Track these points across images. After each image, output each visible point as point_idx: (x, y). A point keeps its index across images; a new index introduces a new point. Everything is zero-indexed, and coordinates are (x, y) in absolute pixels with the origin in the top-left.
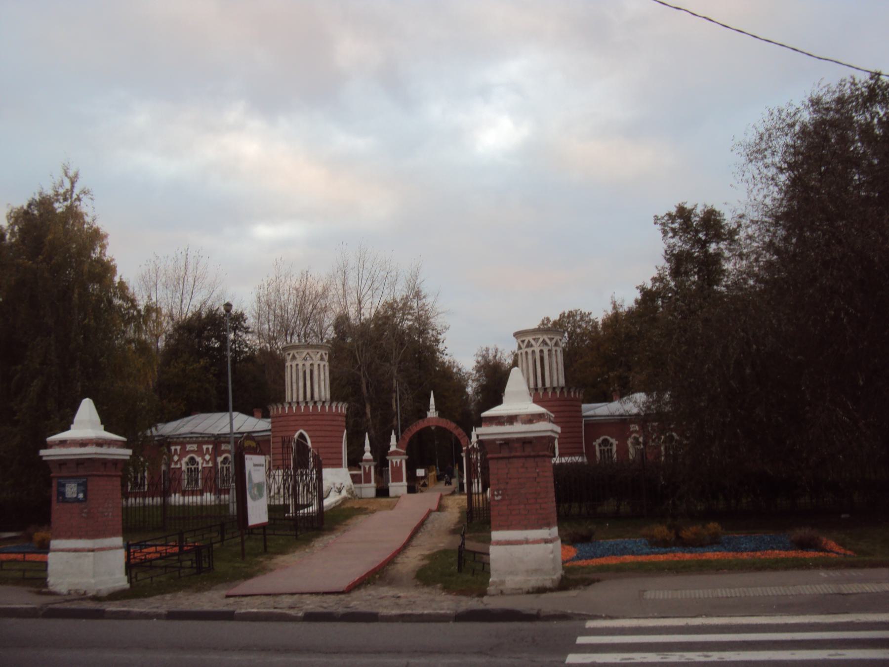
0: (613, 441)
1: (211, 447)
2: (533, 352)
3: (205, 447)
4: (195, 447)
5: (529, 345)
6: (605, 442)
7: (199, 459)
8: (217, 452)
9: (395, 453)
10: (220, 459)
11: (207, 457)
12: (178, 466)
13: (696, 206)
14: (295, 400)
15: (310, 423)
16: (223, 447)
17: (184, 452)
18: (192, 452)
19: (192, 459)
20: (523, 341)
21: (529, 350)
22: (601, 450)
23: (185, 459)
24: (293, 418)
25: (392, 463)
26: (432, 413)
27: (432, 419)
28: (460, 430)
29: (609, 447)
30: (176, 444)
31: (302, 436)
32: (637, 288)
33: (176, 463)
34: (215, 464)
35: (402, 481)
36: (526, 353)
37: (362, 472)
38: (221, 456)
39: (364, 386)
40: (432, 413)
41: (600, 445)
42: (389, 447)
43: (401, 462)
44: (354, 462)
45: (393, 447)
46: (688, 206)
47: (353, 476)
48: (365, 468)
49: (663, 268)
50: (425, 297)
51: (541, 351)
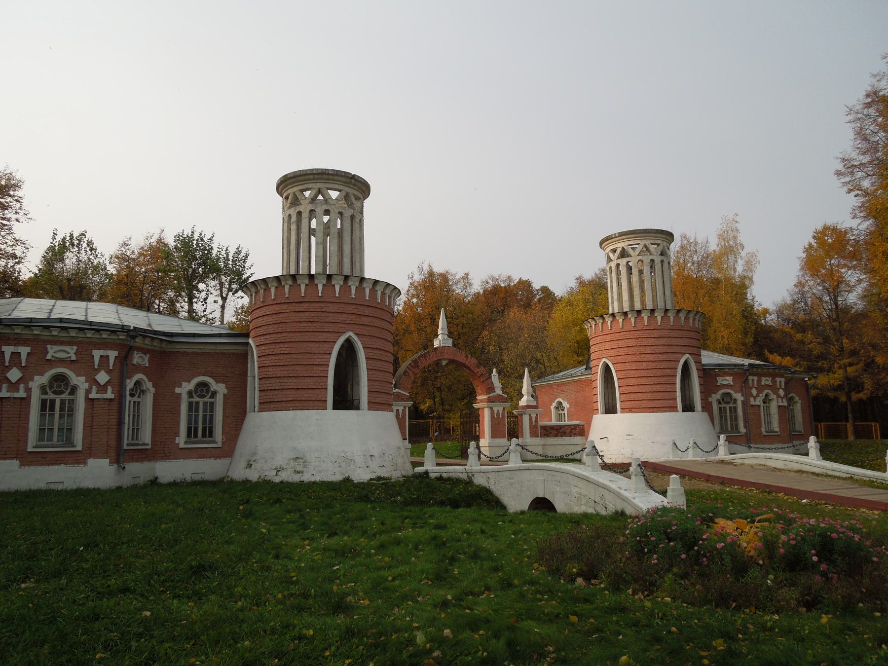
1: (113, 354)
2: (652, 261)
3: (97, 354)
4: (71, 352)
7: (80, 381)
8: (124, 366)
11: (102, 377)
12: (22, 394)
15: (365, 321)
17: (39, 362)
18: (62, 362)
19: (60, 379)
20: (614, 251)
23: (43, 379)
27: (442, 349)
30: (19, 341)
31: (349, 343)
33: (14, 386)
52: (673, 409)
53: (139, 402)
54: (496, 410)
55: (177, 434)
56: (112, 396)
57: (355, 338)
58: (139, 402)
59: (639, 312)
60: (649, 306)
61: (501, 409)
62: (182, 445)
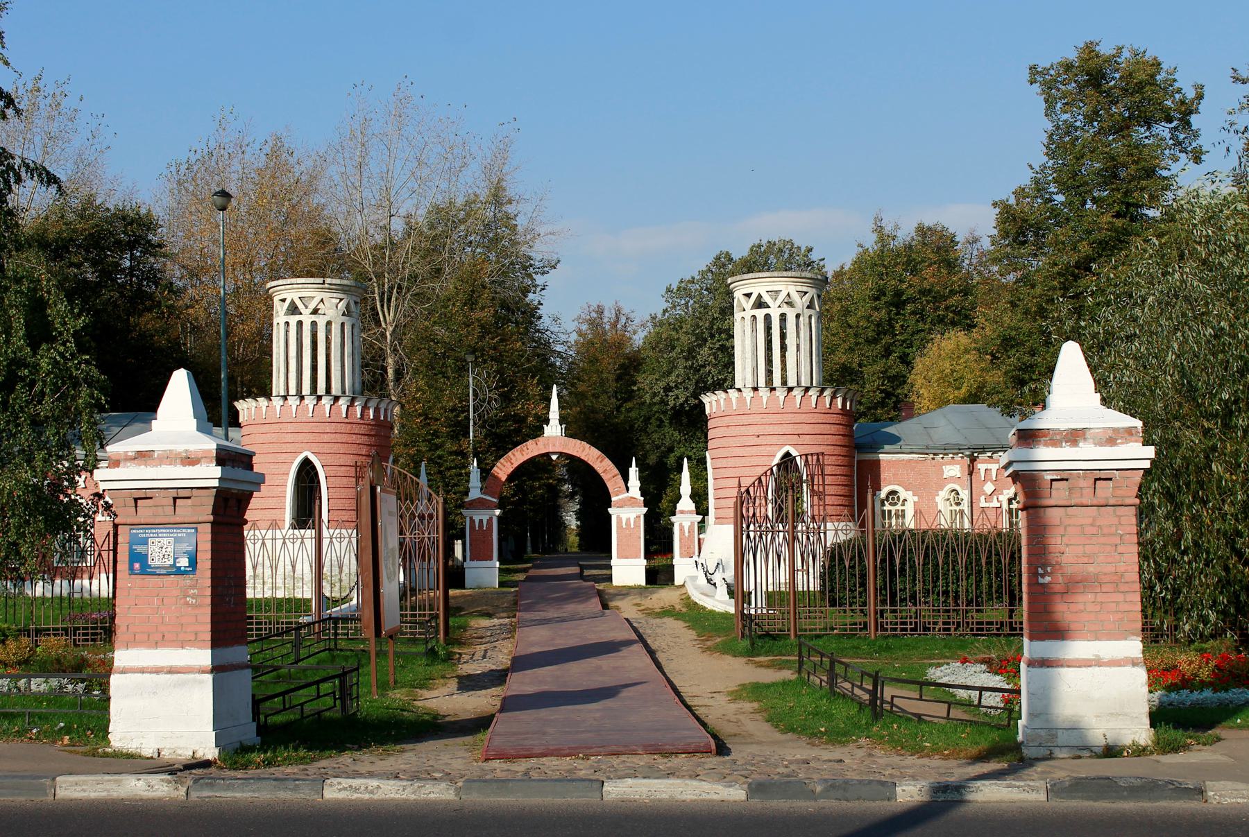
0: (903, 493)
5: (760, 304)
13: (1120, 49)
14: (293, 391)
21: (759, 314)
24: (290, 428)
25: (472, 521)
26: (554, 429)
28: (608, 462)
29: (899, 507)
32: (995, 205)
35: (491, 559)
39: (390, 371)
40: (554, 429)
46: (1106, 49)
49: (1044, 167)
50: (510, 202)
51: (783, 317)
54: (624, 517)
57: (313, 458)
61: (632, 516)
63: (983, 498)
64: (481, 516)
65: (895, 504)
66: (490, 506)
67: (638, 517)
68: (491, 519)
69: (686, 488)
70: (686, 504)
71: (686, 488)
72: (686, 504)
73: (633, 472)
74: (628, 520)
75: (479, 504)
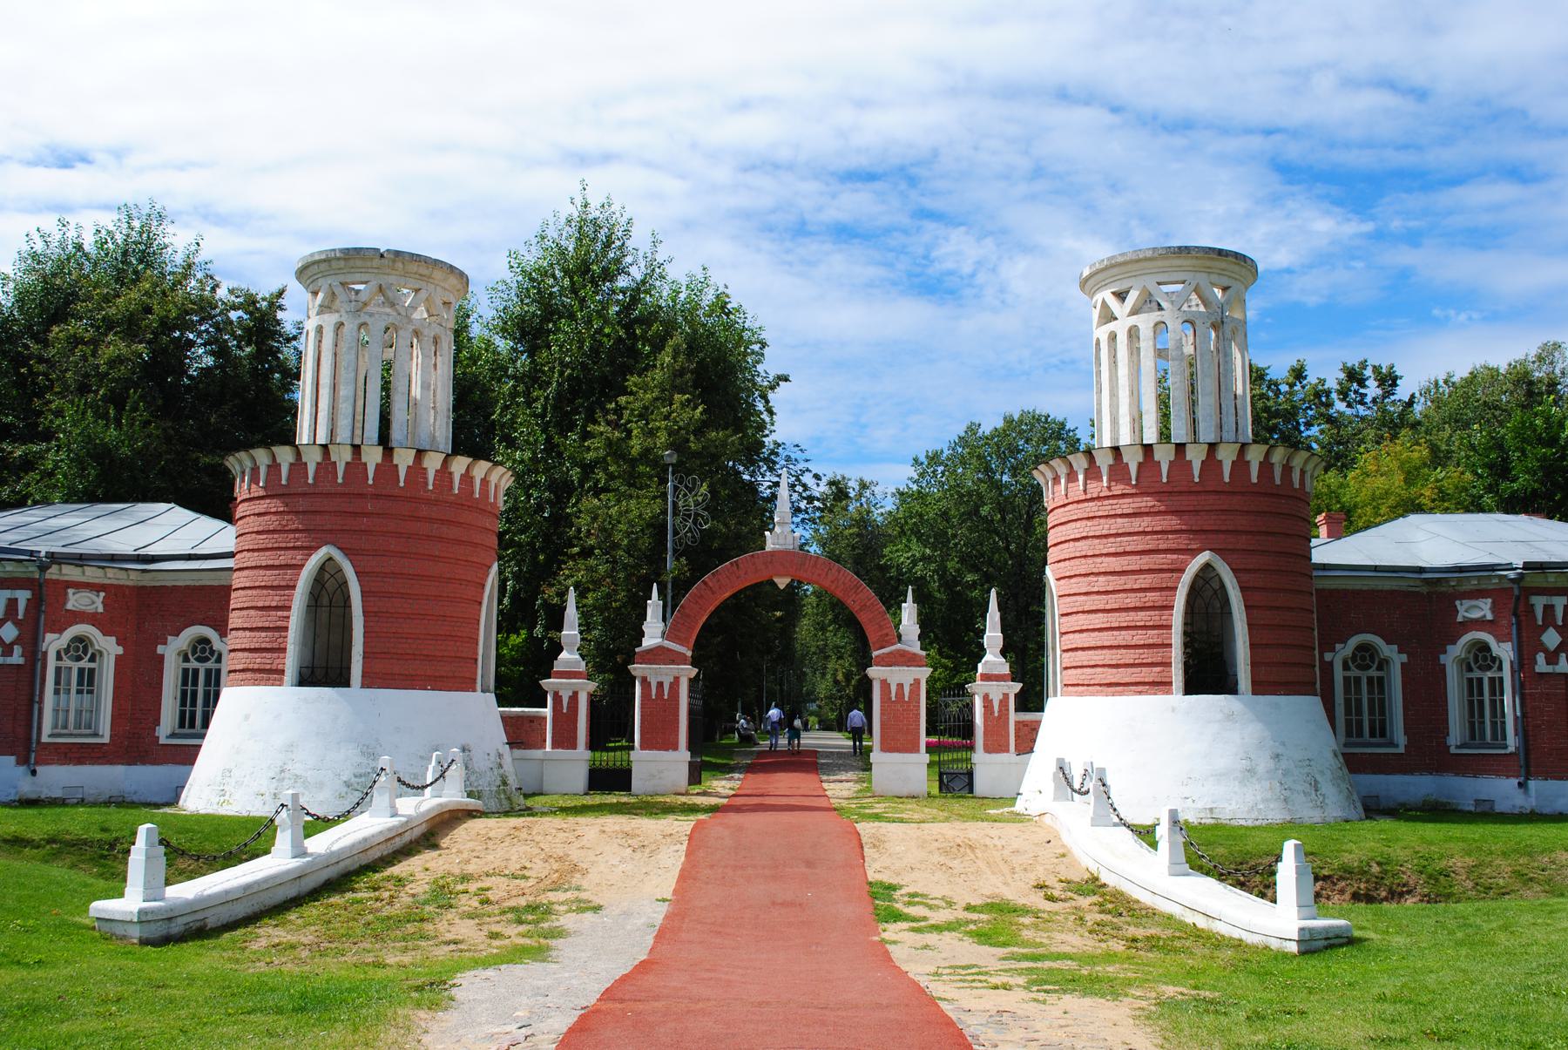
0: (1388, 651)
1: (23, 596)
6: (1365, 654)
9: (657, 655)
10: (54, 643)
16: (76, 601)
22: (1346, 680)
29: (1373, 673)
31: (326, 566)
34: (35, 656)
36: (1133, 333)
37: (547, 712)
38: (60, 631)
41: (1346, 667)
42: (642, 634)
43: (675, 684)
44: (521, 681)
45: (653, 633)
47: (506, 719)
48: (557, 698)
52: (1163, 685)
53: (92, 671)
55: (157, 722)
56: (21, 661)
58: (92, 671)
59: (1180, 447)
60: (1207, 434)
62: (162, 741)
63: (1541, 658)
64: (659, 674)
65: (1369, 667)
66: (675, 658)
67: (917, 682)
68: (677, 679)
69: (993, 636)
70: (993, 660)
71: (993, 636)
72: (993, 660)
73: (909, 613)
74: (900, 686)
75: (657, 655)
